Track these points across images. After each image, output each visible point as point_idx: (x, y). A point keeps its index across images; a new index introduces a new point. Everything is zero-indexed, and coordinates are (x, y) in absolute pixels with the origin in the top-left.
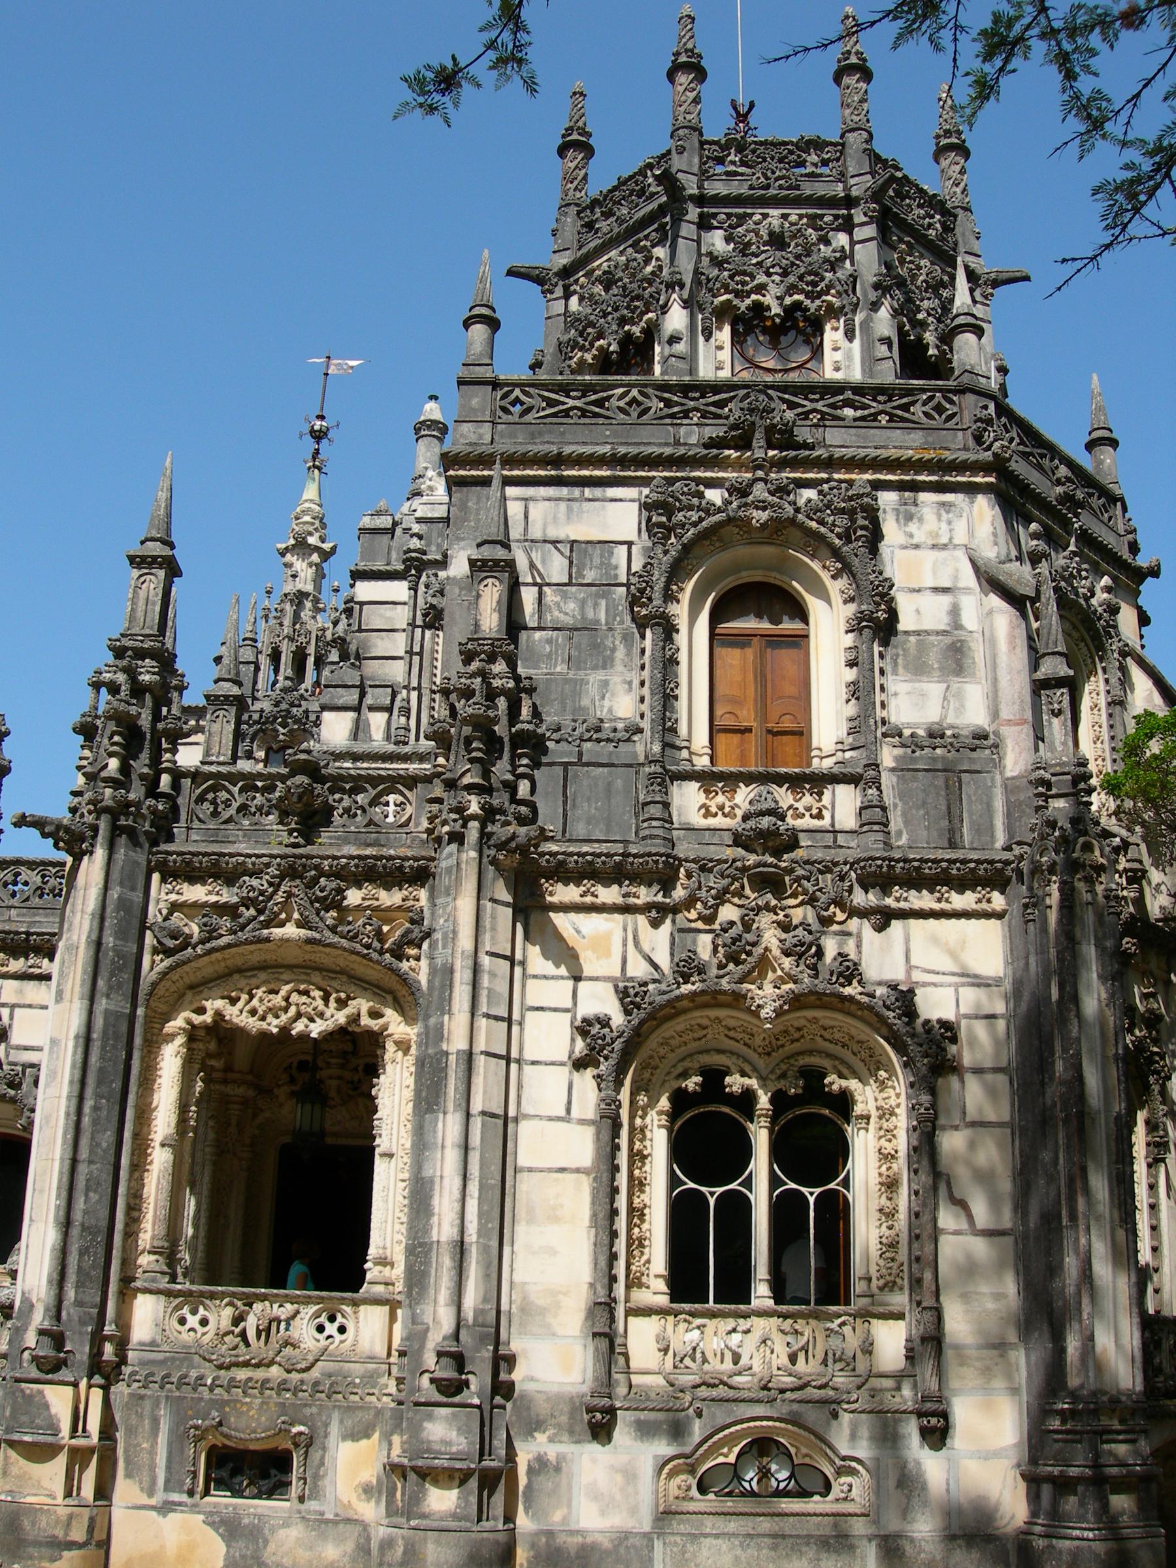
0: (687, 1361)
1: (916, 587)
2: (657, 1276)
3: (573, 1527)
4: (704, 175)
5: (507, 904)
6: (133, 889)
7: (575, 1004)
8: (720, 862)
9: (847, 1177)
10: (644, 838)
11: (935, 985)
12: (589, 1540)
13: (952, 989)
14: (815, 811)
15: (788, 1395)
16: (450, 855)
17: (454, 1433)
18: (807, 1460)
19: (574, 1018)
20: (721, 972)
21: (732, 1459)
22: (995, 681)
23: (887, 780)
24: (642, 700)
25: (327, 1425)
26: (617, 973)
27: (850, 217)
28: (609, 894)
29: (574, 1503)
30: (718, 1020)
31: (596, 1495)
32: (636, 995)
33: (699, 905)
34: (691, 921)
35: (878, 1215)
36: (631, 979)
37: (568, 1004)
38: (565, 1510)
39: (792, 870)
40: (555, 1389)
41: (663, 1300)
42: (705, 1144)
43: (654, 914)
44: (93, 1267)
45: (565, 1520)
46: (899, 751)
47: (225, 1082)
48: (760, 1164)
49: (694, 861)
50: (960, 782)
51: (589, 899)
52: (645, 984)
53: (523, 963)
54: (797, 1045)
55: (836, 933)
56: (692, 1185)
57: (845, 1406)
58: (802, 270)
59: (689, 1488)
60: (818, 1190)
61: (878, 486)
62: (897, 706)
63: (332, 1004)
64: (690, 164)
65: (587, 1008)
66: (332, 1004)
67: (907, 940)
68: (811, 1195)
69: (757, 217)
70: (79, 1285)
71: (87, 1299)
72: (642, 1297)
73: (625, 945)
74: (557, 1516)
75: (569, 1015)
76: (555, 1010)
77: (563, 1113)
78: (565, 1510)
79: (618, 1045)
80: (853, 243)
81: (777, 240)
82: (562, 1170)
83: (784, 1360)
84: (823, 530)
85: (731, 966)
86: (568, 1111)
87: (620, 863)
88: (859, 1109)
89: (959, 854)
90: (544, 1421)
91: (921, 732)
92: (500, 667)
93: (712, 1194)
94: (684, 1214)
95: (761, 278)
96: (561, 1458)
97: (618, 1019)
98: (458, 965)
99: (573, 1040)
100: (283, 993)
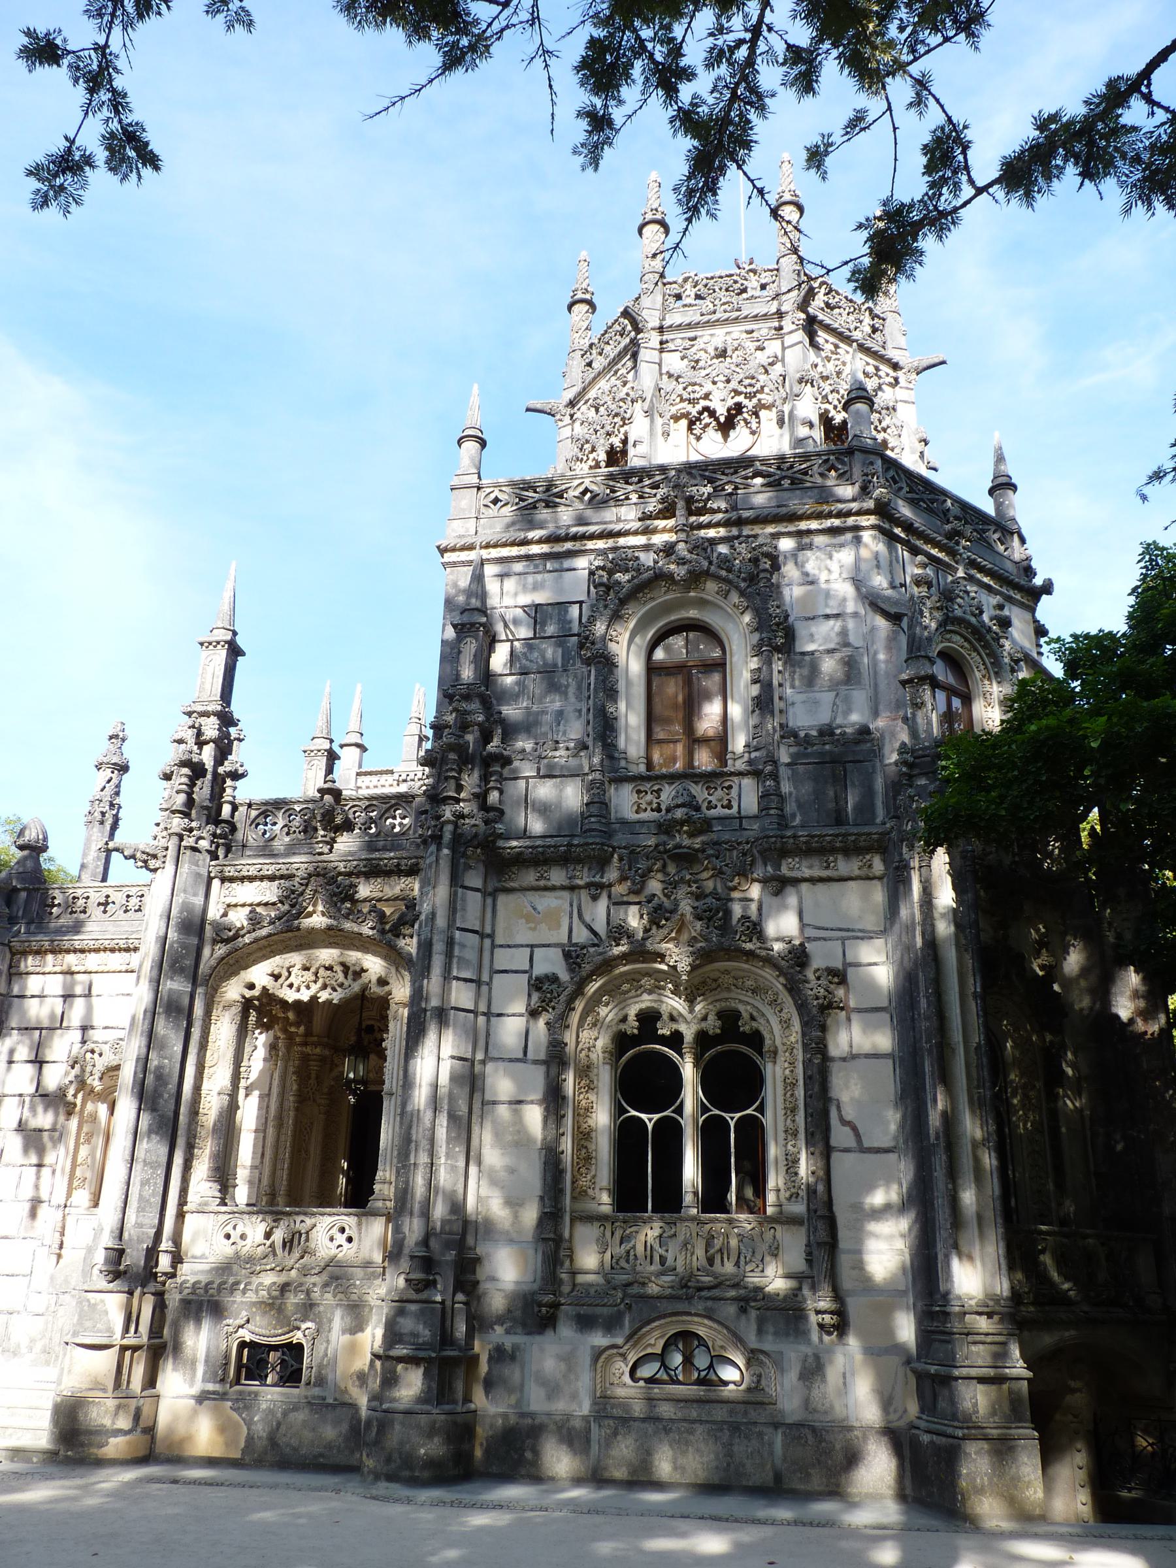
0: (623, 1263)
1: (811, 615)
4: (665, 309)
5: (477, 890)
6: (195, 895)
7: (531, 966)
9: (762, 1103)
10: (585, 832)
11: (825, 939)
12: (537, 1421)
15: (704, 1293)
16: (432, 853)
17: (421, 1327)
19: (530, 977)
22: (876, 685)
23: (784, 772)
24: (588, 722)
25: (330, 1321)
26: (565, 941)
27: (781, 328)
28: (557, 876)
29: (526, 1387)
32: (578, 957)
36: (576, 945)
37: (527, 968)
38: (518, 1395)
39: (703, 851)
44: (153, 1195)
46: (793, 750)
47: (305, 1044)
48: (691, 1094)
49: (625, 848)
50: (845, 771)
51: (542, 883)
52: (583, 948)
53: (491, 936)
57: (753, 1304)
58: (741, 376)
61: (776, 536)
62: (794, 713)
63: (350, 976)
64: (654, 302)
65: (539, 970)
66: (350, 976)
69: (706, 339)
70: (141, 1210)
71: (147, 1221)
76: (516, 972)
77: (521, 1055)
80: (784, 349)
81: (722, 354)
83: (704, 1262)
84: (731, 576)
86: (525, 1053)
87: (565, 852)
89: (842, 830)
91: (814, 733)
92: (475, 705)
95: (708, 387)
96: (516, 1348)
97: (564, 976)
98: (435, 938)
99: (529, 995)
100: (313, 970)
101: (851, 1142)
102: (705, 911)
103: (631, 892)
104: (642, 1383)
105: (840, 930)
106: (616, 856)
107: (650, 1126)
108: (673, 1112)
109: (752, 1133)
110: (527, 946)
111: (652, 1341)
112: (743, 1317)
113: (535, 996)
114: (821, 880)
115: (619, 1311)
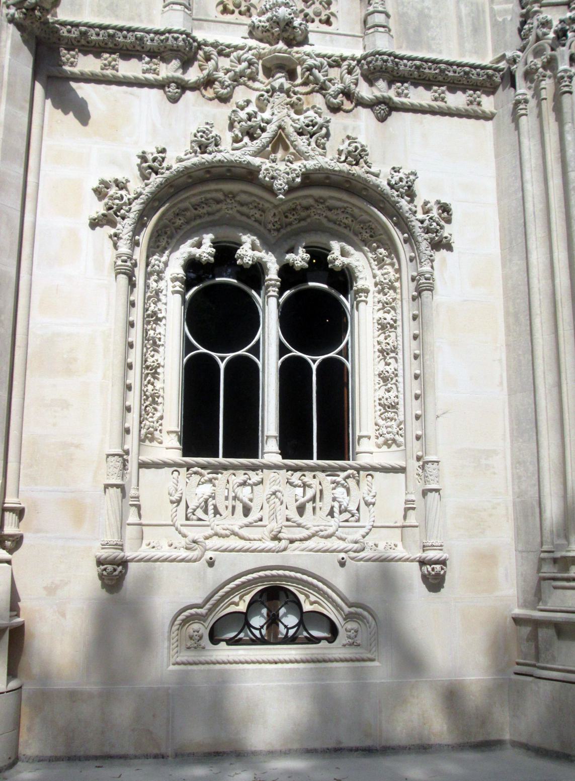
0: (200, 513)
2: (169, 432)
8: (237, 48)
14: (323, 17)
15: (297, 544)
20: (236, 145)
21: (242, 607)
30: (233, 195)
32: (154, 160)
33: (217, 85)
35: (377, 379)
41: (176, 455)
42: (218, 309)
43: (173, 89)
54: (303, 224)
56: (203, 350)
59: (201, 637)
60: (320, 358)
68: (314, 362)
72: (155, 453)
79: (136, 206)
85: (246, 139)
88: (359, 284)
94: (197, 376)
102: (308, 126)
107: (222, 366)
108: (247, 351)
109: (336, 379)
111: (236, 599)
114: (432, 112)
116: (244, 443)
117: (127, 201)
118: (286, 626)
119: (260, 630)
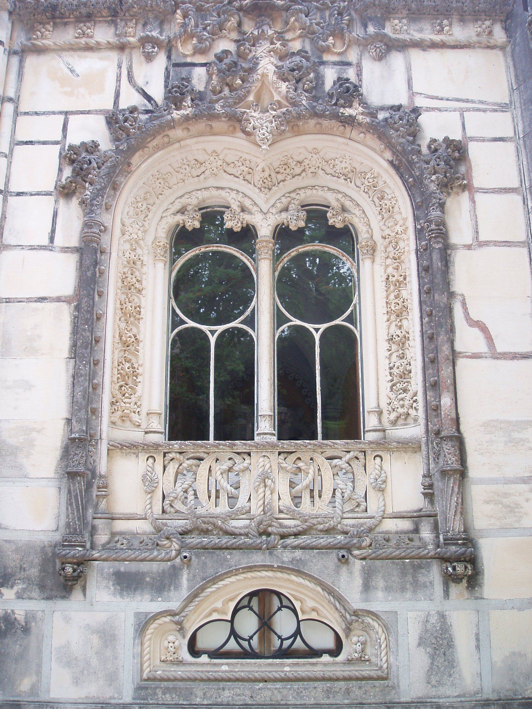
3: (43, 697)
7: (65, 136)
11: (440, 110)
13: (457, 114)
15: (290, 541)
18: (314, 616)
19: (63, 149)
26: (110, 106)
28: (103, 34)
29: (45, 669)
31: (69, 661)
34: (185, 56)
37: (59, 137)
38: (34, 678)
40: (25, 538)
45: (34, 689)
48: (265, 299)
53: (15, 101)
55: (335, 64)
56: (191, 324)
57: (356, 552)
60: (323, 327)
65: (76, 138)
67: (409, 69)
68: (317, 330)
73: (119, 80)
74: (25, 685)
75: (58, 147)
77: (45, 241)
78: (34, 678)
82: (42, 299)
83: (287, 501)
86: (52, 239)
90: (12, 575)
93: (213, 333)
96: (30, 617)
97: (106, 144)
99: (60, 170)
101: (482, 347)
103: (198, 51)
104: (204, 658)
105: (458, 100)
106: (178, 11)
108: (242, 322)
109: (344, 349)
110: (61, 113)
111: (219, 605)
112: (344, 569)
113: (68, 172)
114: (434, 45)
115: (174, 567)
116: (236, 425)
117: (96, 165)
118: (279, 637)
119: (249, 641)
